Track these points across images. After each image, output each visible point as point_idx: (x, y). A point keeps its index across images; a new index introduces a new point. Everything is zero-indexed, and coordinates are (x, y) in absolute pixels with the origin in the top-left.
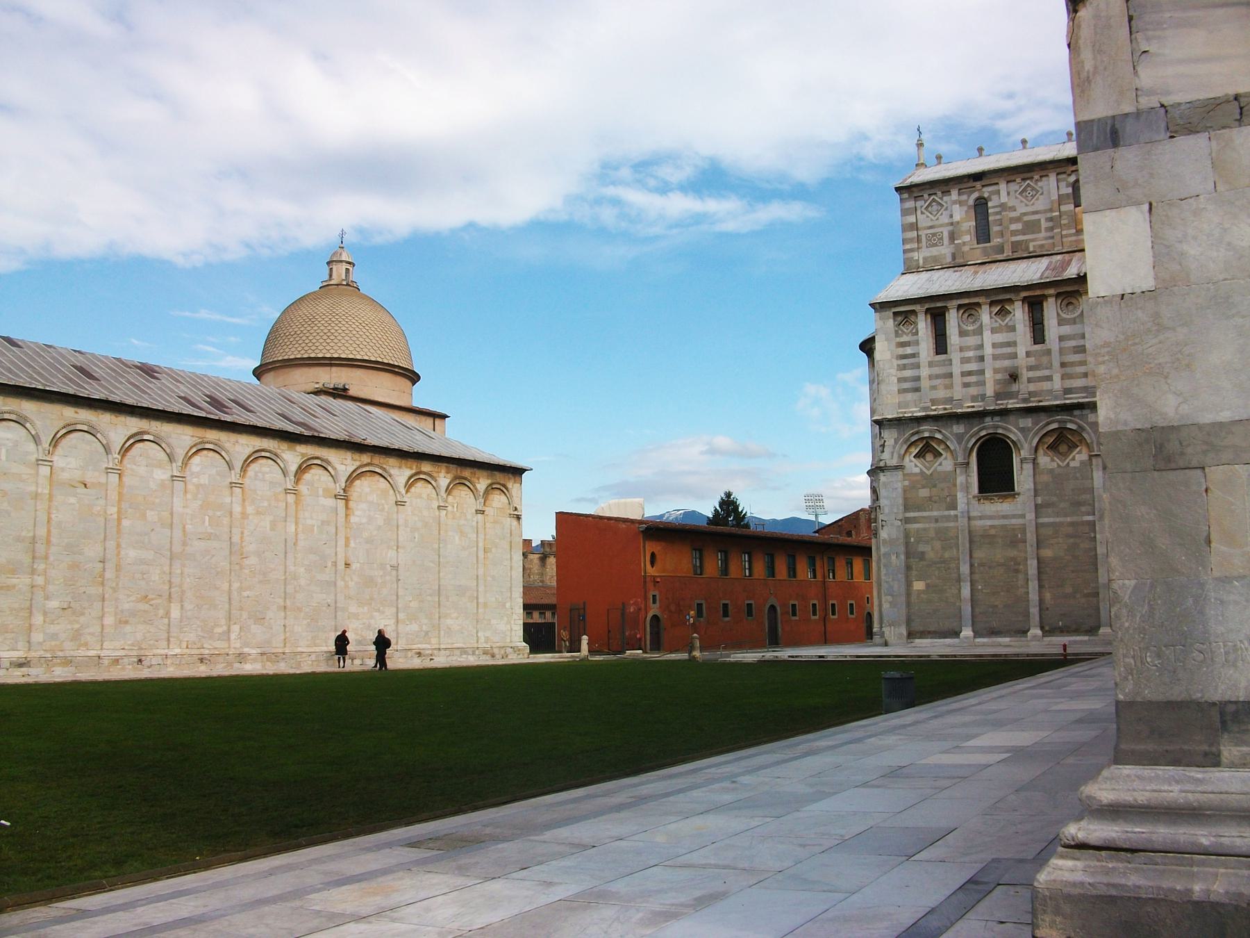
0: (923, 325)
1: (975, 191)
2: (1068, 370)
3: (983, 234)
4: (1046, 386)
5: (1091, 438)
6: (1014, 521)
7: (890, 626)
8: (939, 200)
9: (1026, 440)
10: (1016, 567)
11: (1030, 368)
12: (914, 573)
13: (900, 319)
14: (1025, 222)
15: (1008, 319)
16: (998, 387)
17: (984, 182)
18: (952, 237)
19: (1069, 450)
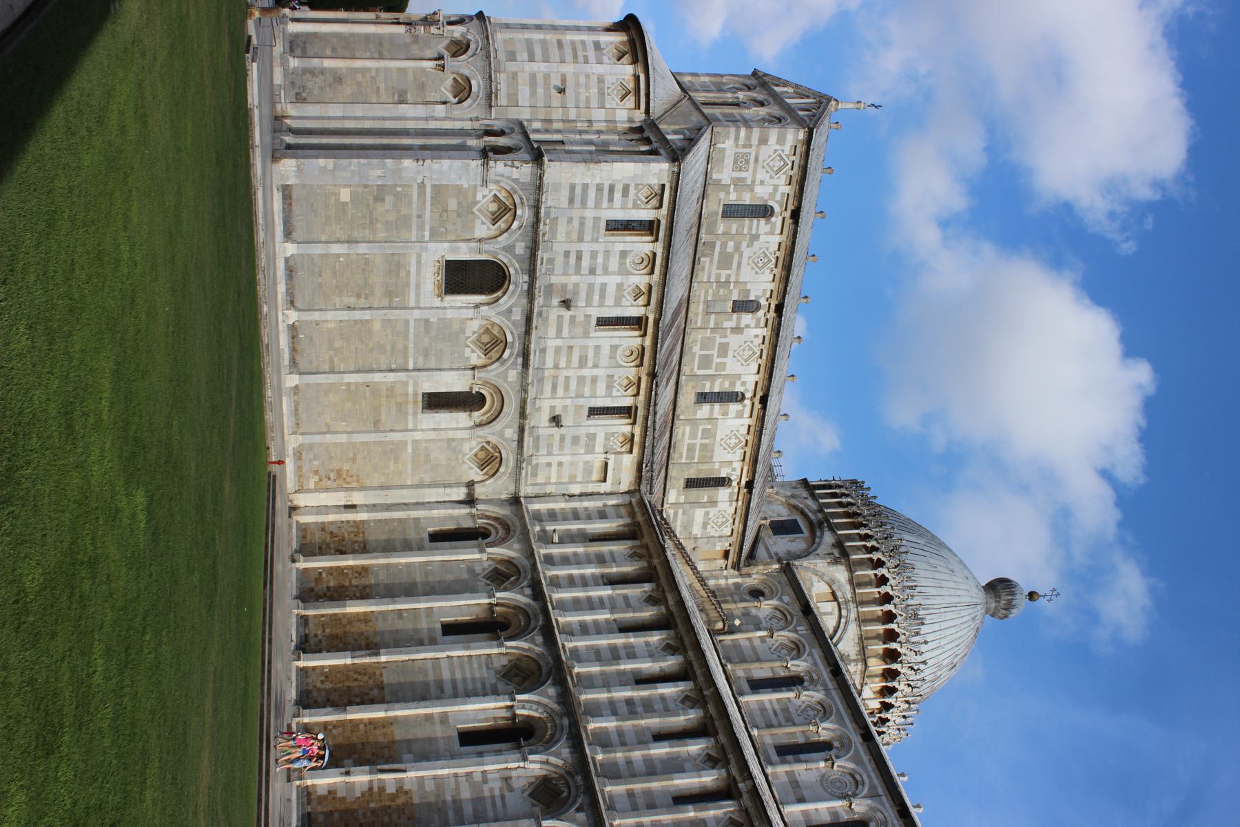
0: (646, 214)
1: (781, 208)
2: (564, 352)
3: (732, 211)
4: (552, 331)
5: (492, 371)
6: (413, 294)
7: (298, 166)
8: (784, 170)
9: (498, 314)
10: (363, 296)
11: (573, 318)
12: (360, 190)
13: (657, 189)
14: (733, 255)
15: (628, 297)
16: (560, 286)
17: (788, 221)
18: (739, 183)
19: (483, 343)
